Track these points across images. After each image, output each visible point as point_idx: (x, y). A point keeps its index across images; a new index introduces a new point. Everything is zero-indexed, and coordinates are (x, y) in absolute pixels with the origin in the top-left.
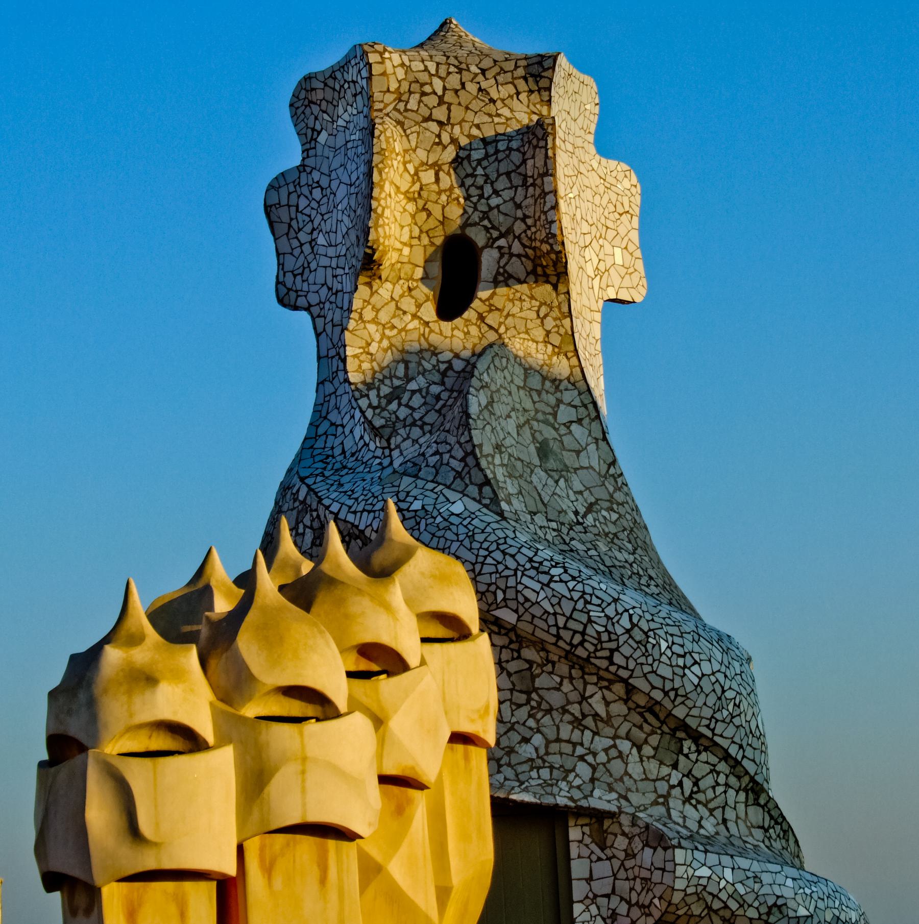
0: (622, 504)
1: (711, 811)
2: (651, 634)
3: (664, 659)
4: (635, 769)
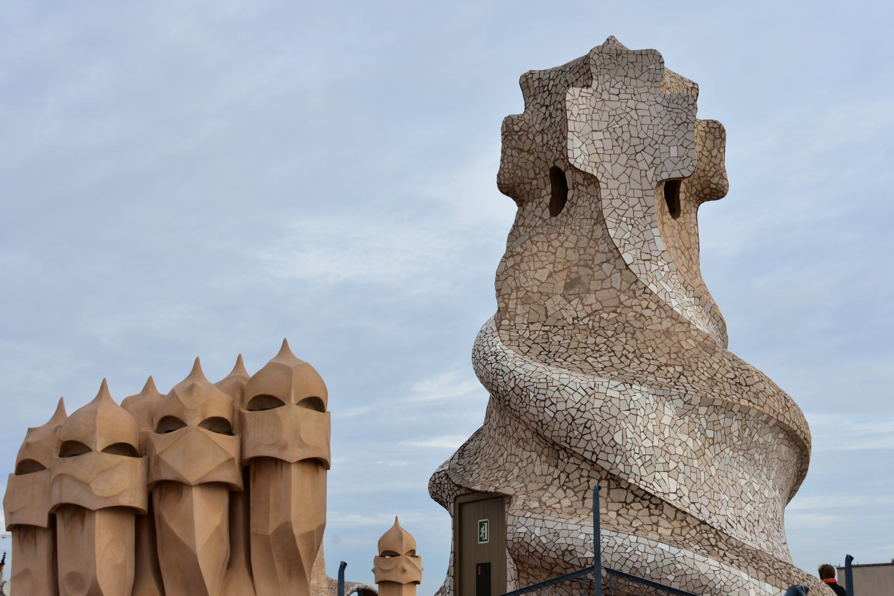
0: (631, 307)
1: (576, 493)
3: (532, 403)
4: (538, 471)
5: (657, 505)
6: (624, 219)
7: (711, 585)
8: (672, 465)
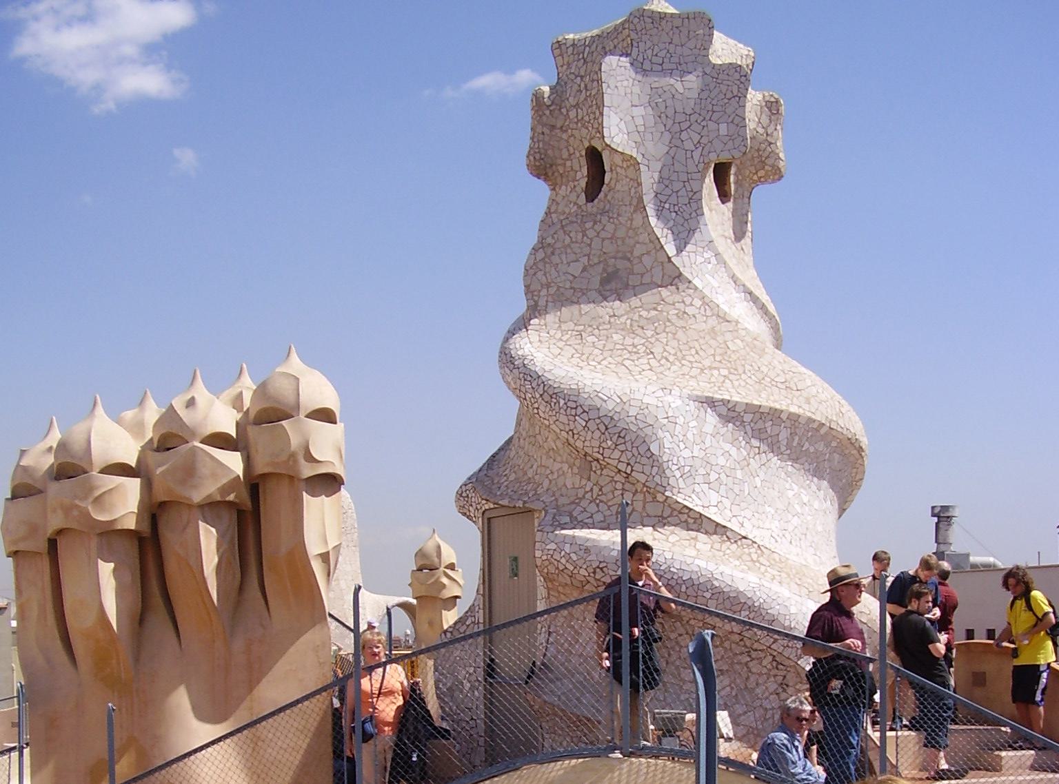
2: (554, 396)
5: (695, 519)
6: (667, 206)
7: (750, 603)
8: (713, 476)
